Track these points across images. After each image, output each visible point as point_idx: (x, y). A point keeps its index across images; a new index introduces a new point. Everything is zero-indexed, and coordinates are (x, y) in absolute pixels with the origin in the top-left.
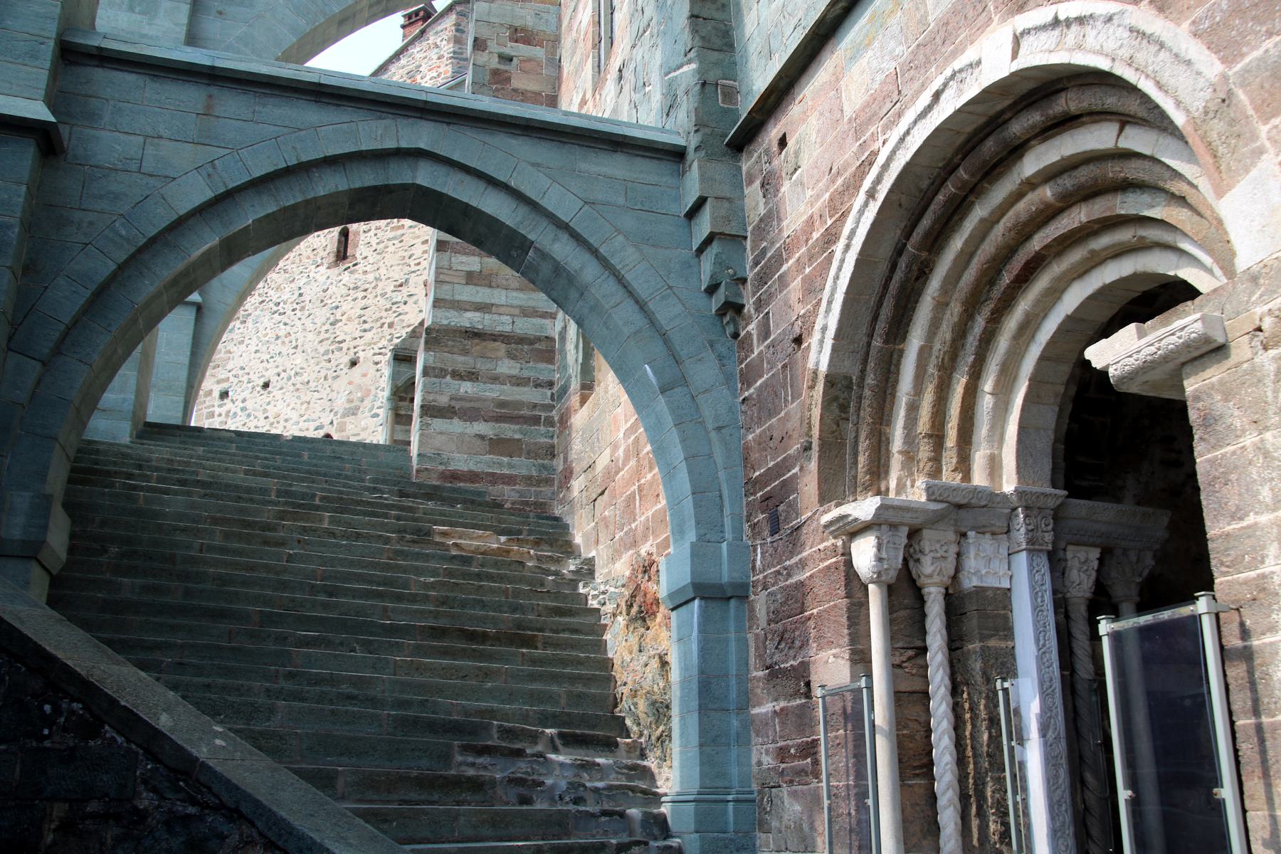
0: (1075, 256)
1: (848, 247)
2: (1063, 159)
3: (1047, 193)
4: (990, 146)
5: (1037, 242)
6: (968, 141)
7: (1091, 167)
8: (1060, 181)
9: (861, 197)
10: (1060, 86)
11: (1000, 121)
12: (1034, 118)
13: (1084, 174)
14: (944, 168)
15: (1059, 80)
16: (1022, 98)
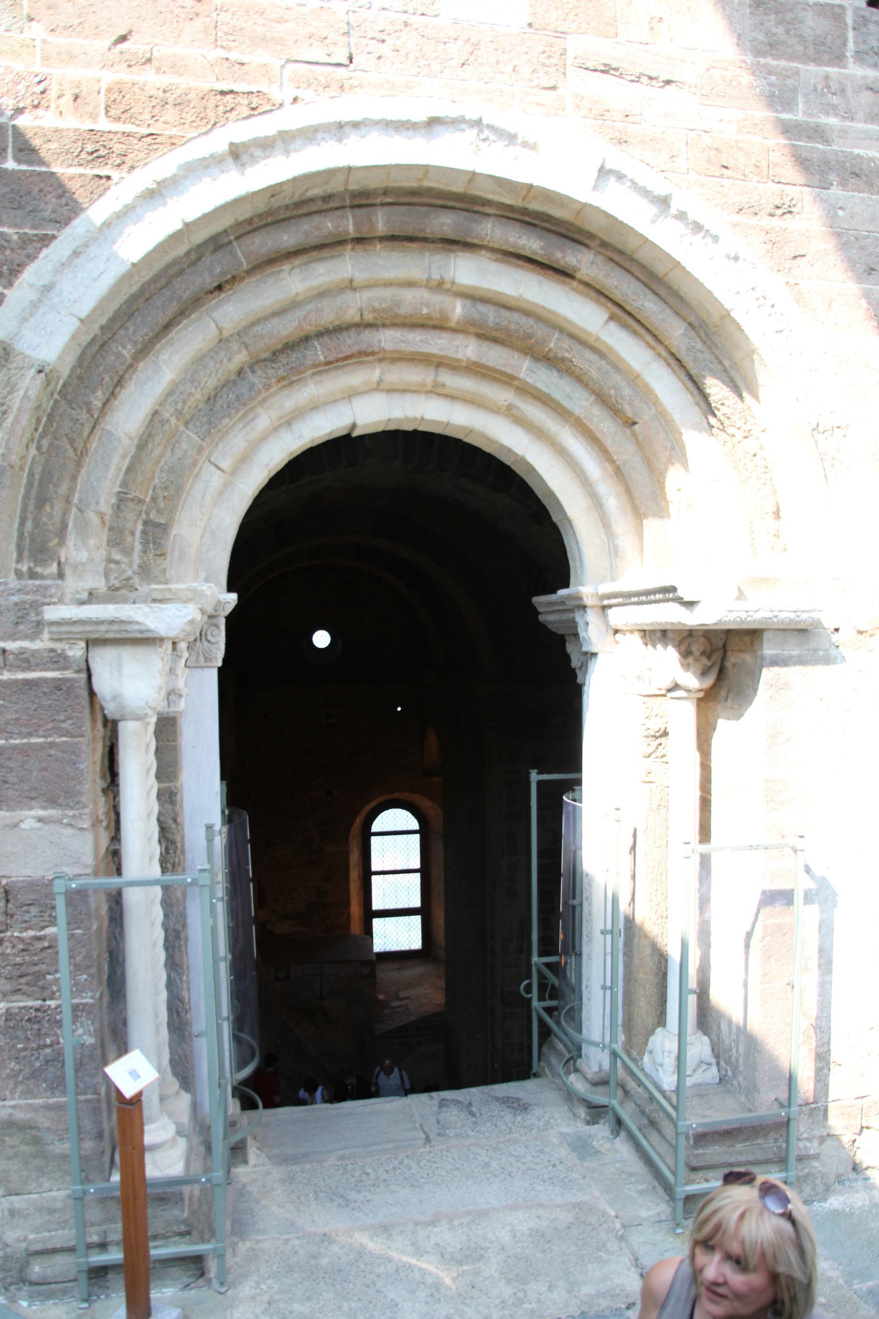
0: (414, 375)
1: (154, 195)
2: (518, 299)
3: (458, 310)
4: (445, 223)
5: (387, 339)
6: (414, 192)
7: (531, 322)
8: (482, 308)
9: (218, 142)
10: (586, 241)
11: (476, 208)
12: (531, 243)
13: (516, 321)
14: (355, 195)
15: (592, 236)
16: (525, 211)
